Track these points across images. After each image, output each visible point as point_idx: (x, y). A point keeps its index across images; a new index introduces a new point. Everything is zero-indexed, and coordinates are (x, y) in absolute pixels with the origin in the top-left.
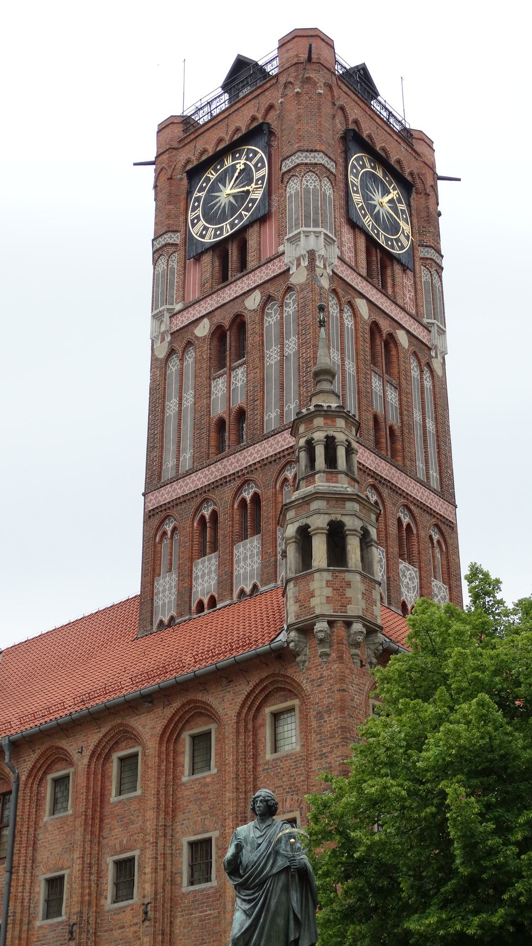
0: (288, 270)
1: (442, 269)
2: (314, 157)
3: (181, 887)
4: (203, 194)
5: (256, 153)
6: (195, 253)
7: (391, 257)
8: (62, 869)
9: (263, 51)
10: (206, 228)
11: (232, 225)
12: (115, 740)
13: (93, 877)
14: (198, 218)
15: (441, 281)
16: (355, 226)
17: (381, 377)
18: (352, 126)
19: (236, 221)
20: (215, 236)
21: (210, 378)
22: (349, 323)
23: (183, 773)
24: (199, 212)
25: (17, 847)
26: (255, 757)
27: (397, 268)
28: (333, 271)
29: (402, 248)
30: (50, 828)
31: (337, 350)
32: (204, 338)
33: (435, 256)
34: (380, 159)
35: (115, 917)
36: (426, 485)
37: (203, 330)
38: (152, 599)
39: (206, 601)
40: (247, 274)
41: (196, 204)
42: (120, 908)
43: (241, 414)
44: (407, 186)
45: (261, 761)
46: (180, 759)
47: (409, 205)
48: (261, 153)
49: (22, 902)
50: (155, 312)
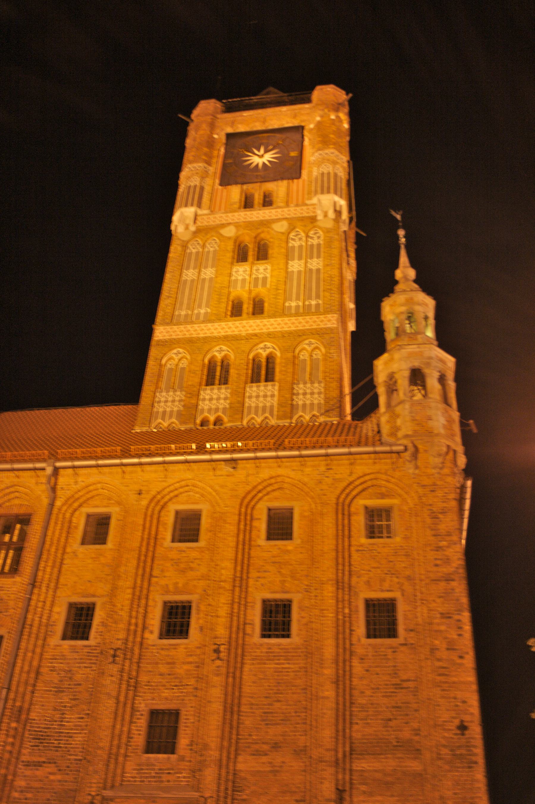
3: (251, 636)
8: (94, 596)
12: (176, 492)
13: (141, 610)
23: (258, 537)
25: (42, 564)
26: (350, 537)
30: (80, 556)
32: (229, 238)
35: (163, 652)
37: (230, 232)
38: (153, 406)
39: (212, 418)
42: (170, 645)
45: (353, 543)
46: (255, 524)
49: (41, 618)
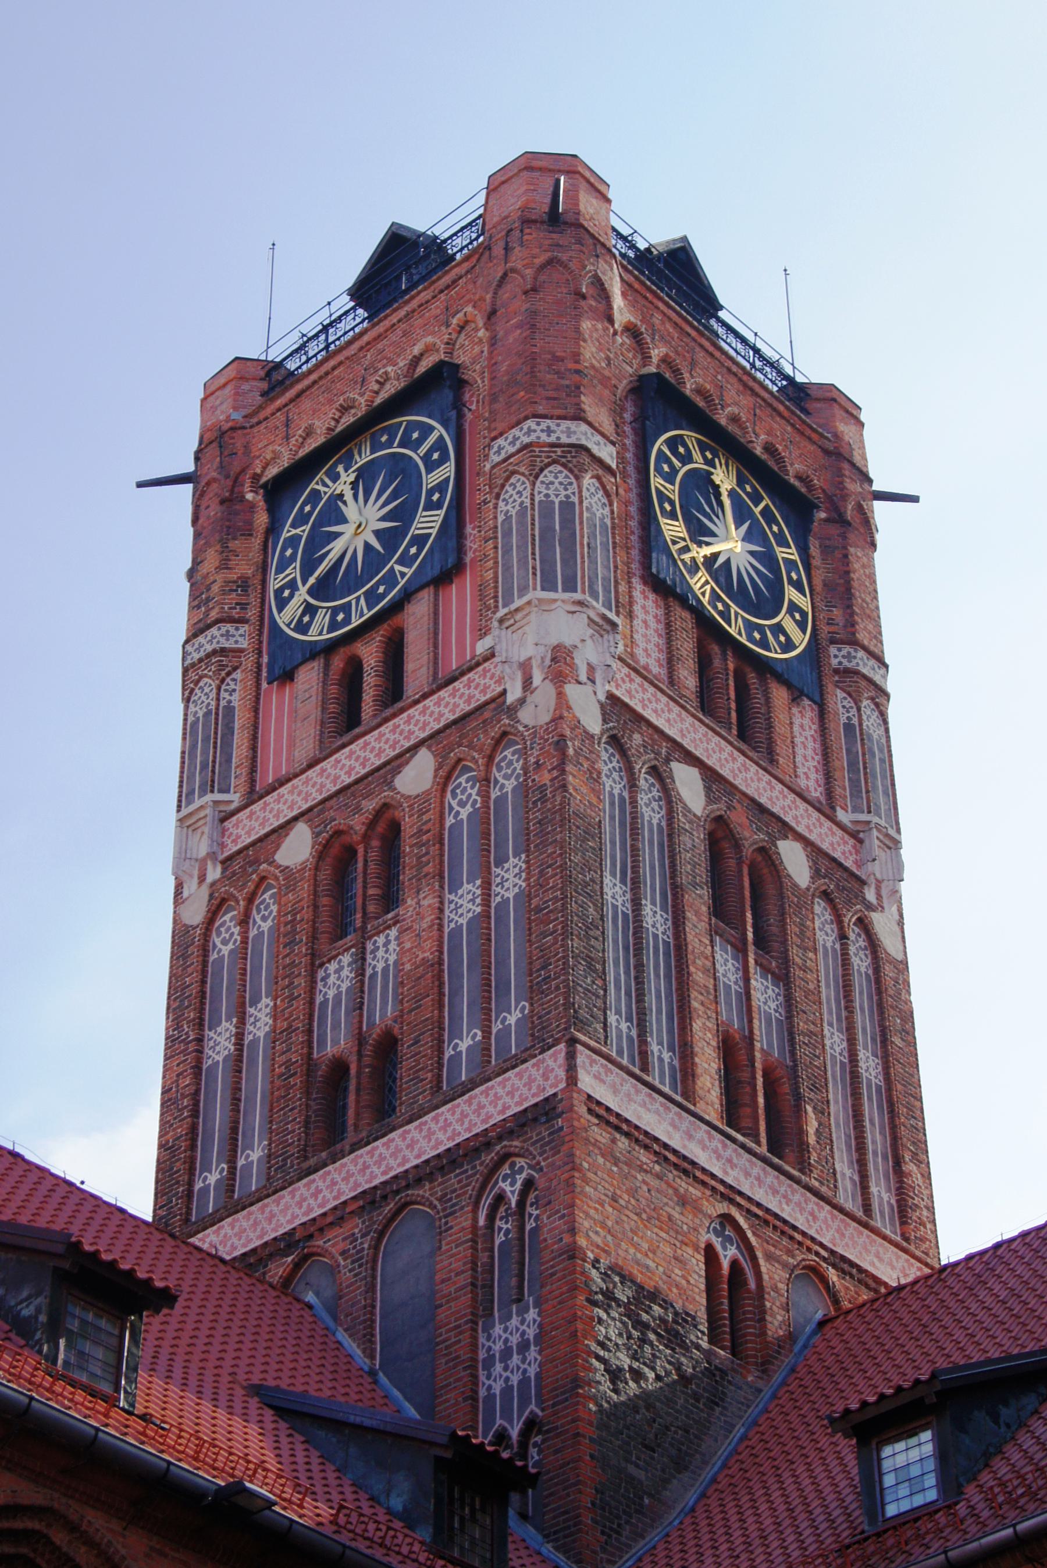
0: (504, 692)
1: (887, 696)
7: (764, 668)
9: (444, 203)
11: (372, 597)
14: (292, 585)
15: (885, 722)
16: (669, 592)
17: (740, 949)
19: (381, 589)
20: (333, 626)
21: (316, 962)
27: (780, 695)
29: (789, 646)
31: (623, 881)
33: (867, 667)
34: (725, 443)
37: (298, 849)
40: (402, 710)
41: (289, 552)
43: (387, 1047)
44: (797, 506)
47: (804, 550)
48: (439, 430)
50: (185, 811)
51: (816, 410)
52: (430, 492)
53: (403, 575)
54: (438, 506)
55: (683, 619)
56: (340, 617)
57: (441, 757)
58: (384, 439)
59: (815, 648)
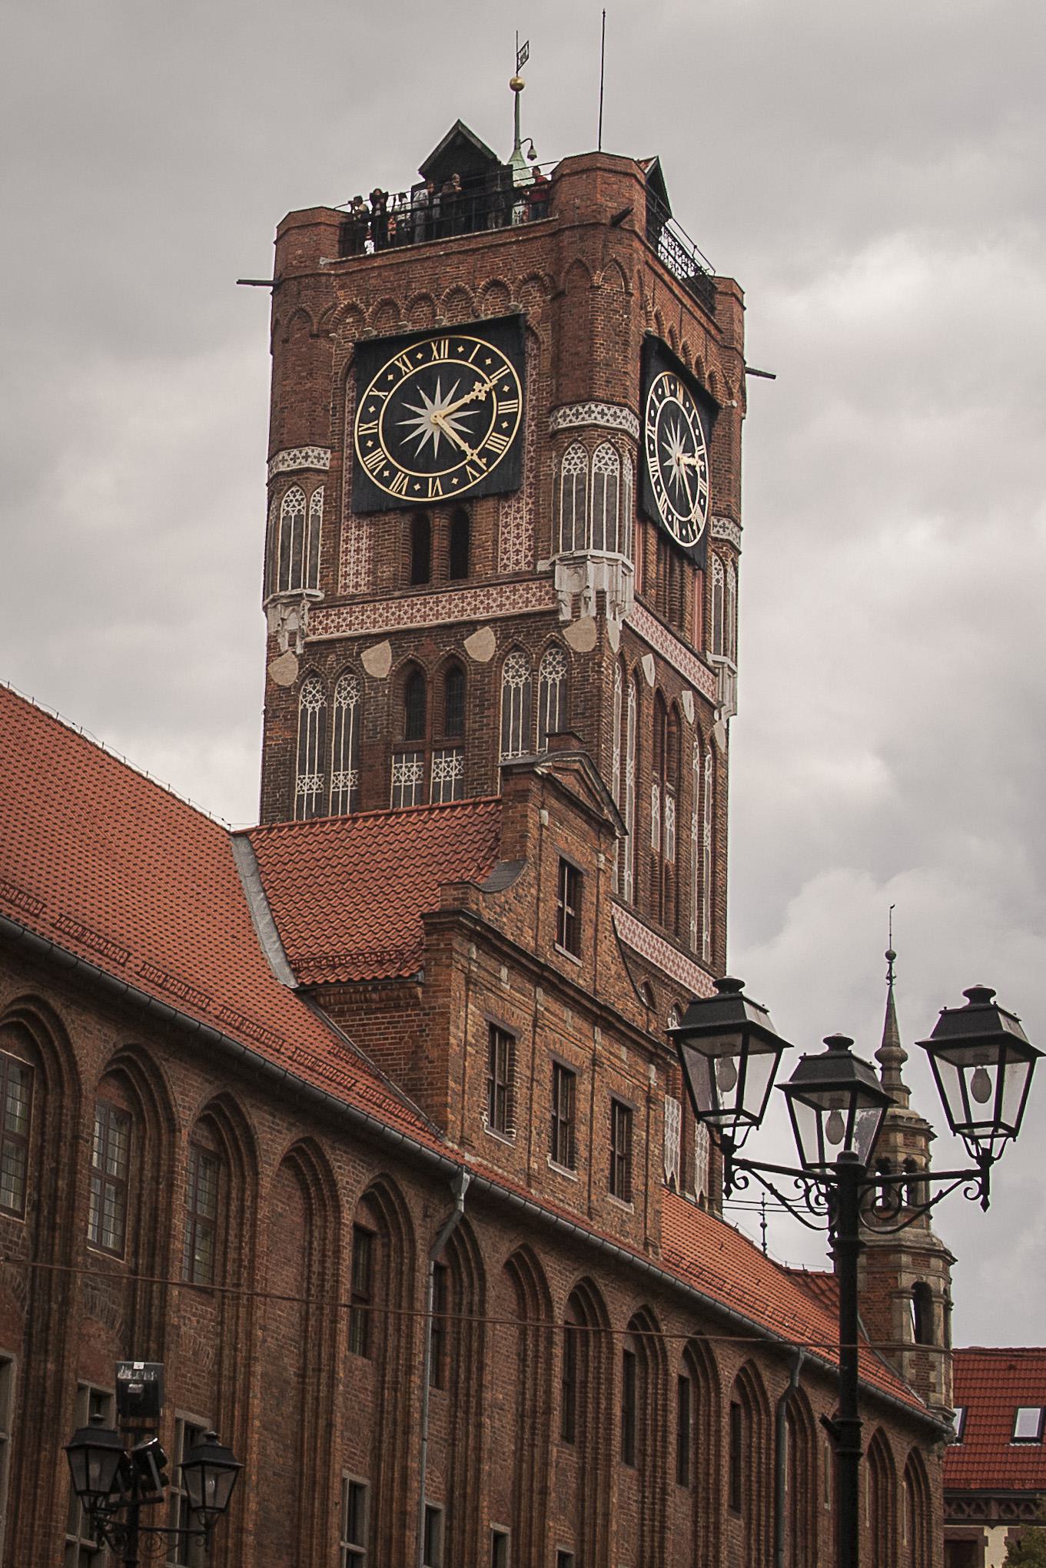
0: (556, 612)
2: (615, 416)
4: (388, 396)
5: (498, 363)
6: (371, 505)
10: (388, 466)
14: (374, 437)
16: (645, 515)
18: (653, 329)
22: (631, 702)
24: (377, 427)
27: (688, 571)
28: (624, 622)
34: (682, 373)
36: (697, 960)
41: (372, 409)
48: (509, 367)
51: (711, 296)
52: (501, 418)
53: (475, 478)
54: (507, 433)
55: (653, 541)
56: (417, 487)
57: (503, 637)
58: (461, 349)
59: (707, 525)
